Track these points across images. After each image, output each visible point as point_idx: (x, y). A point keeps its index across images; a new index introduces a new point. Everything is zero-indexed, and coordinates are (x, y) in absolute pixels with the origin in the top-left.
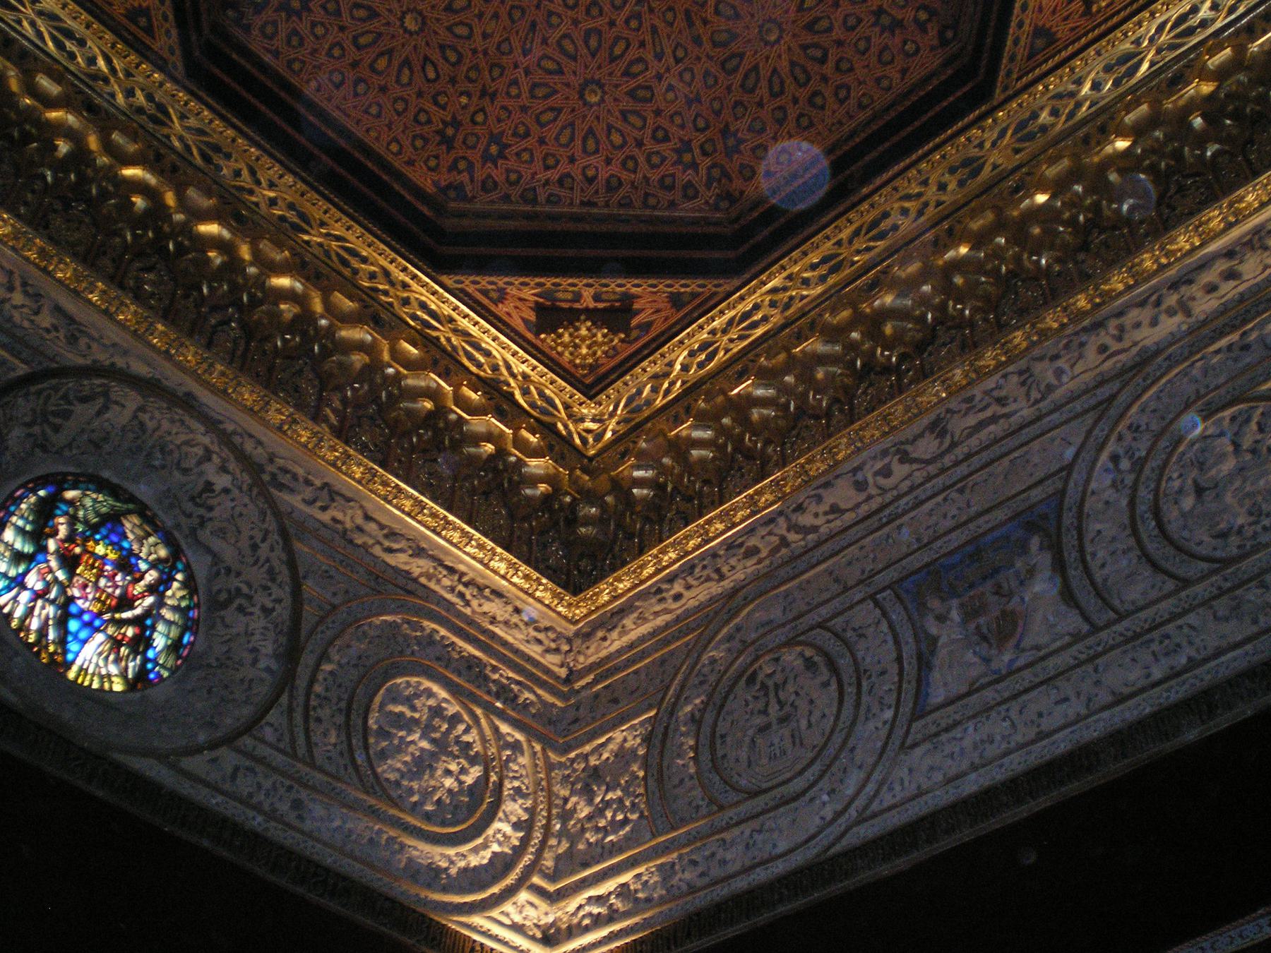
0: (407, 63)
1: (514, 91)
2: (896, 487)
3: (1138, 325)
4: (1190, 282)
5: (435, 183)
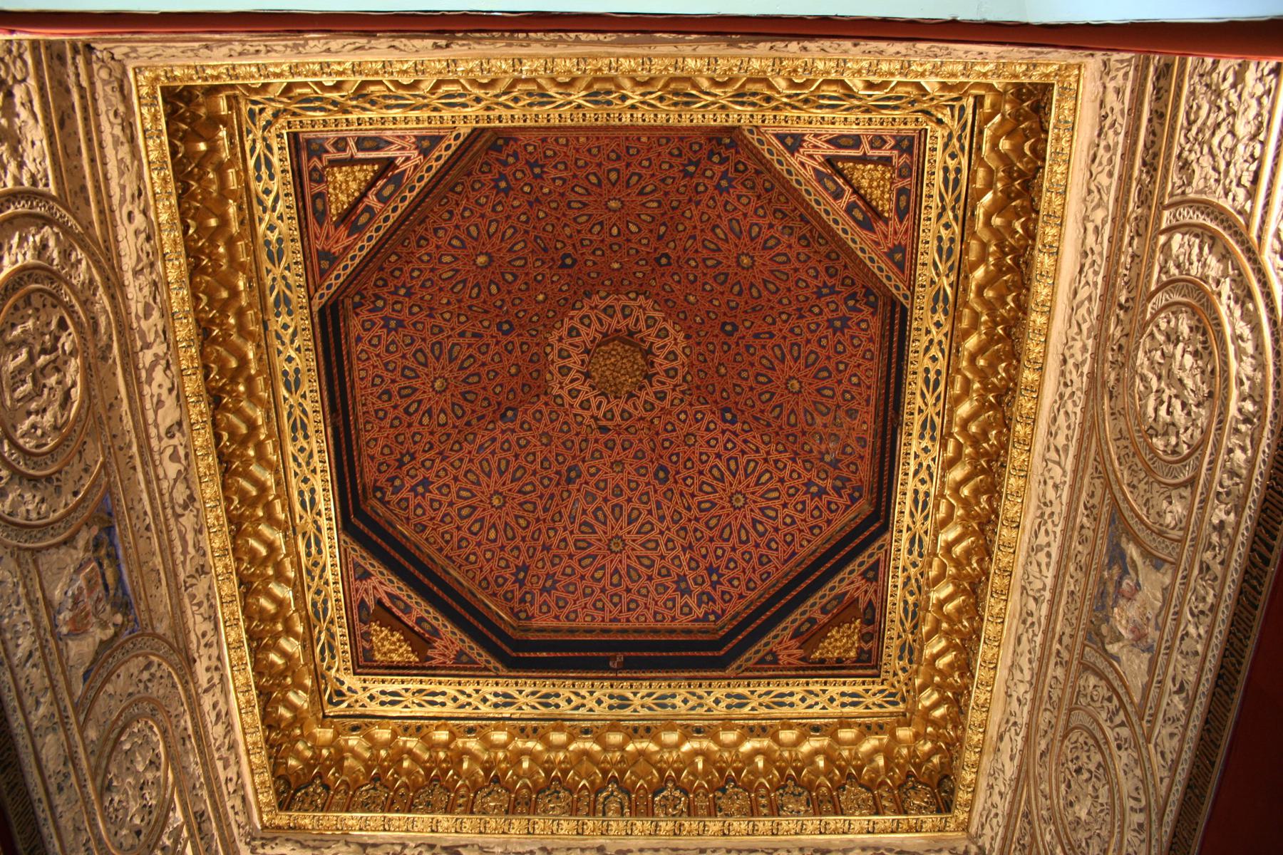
0: (600, 185)
1: (523, 218)
5: (516, 140)
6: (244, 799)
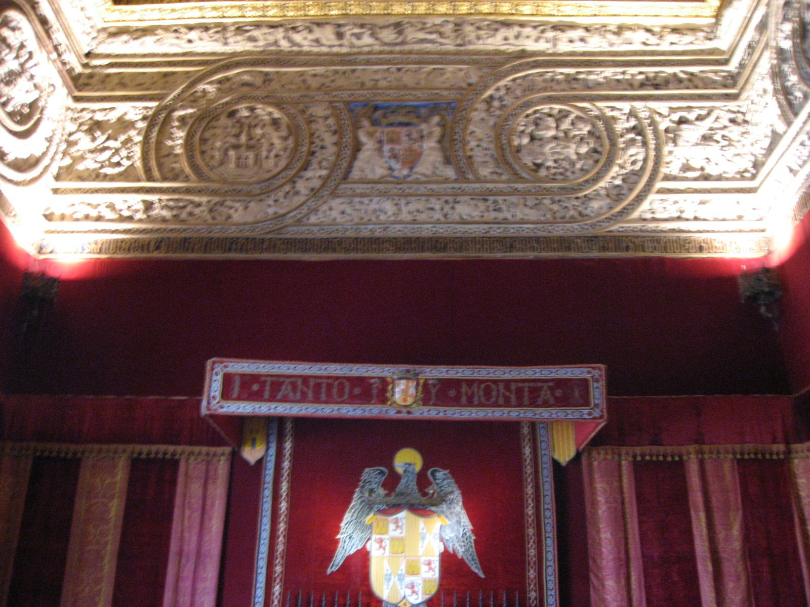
2: (359, 47)
3: (528, 37)
4: (563, 31)
6: (675, 30)
